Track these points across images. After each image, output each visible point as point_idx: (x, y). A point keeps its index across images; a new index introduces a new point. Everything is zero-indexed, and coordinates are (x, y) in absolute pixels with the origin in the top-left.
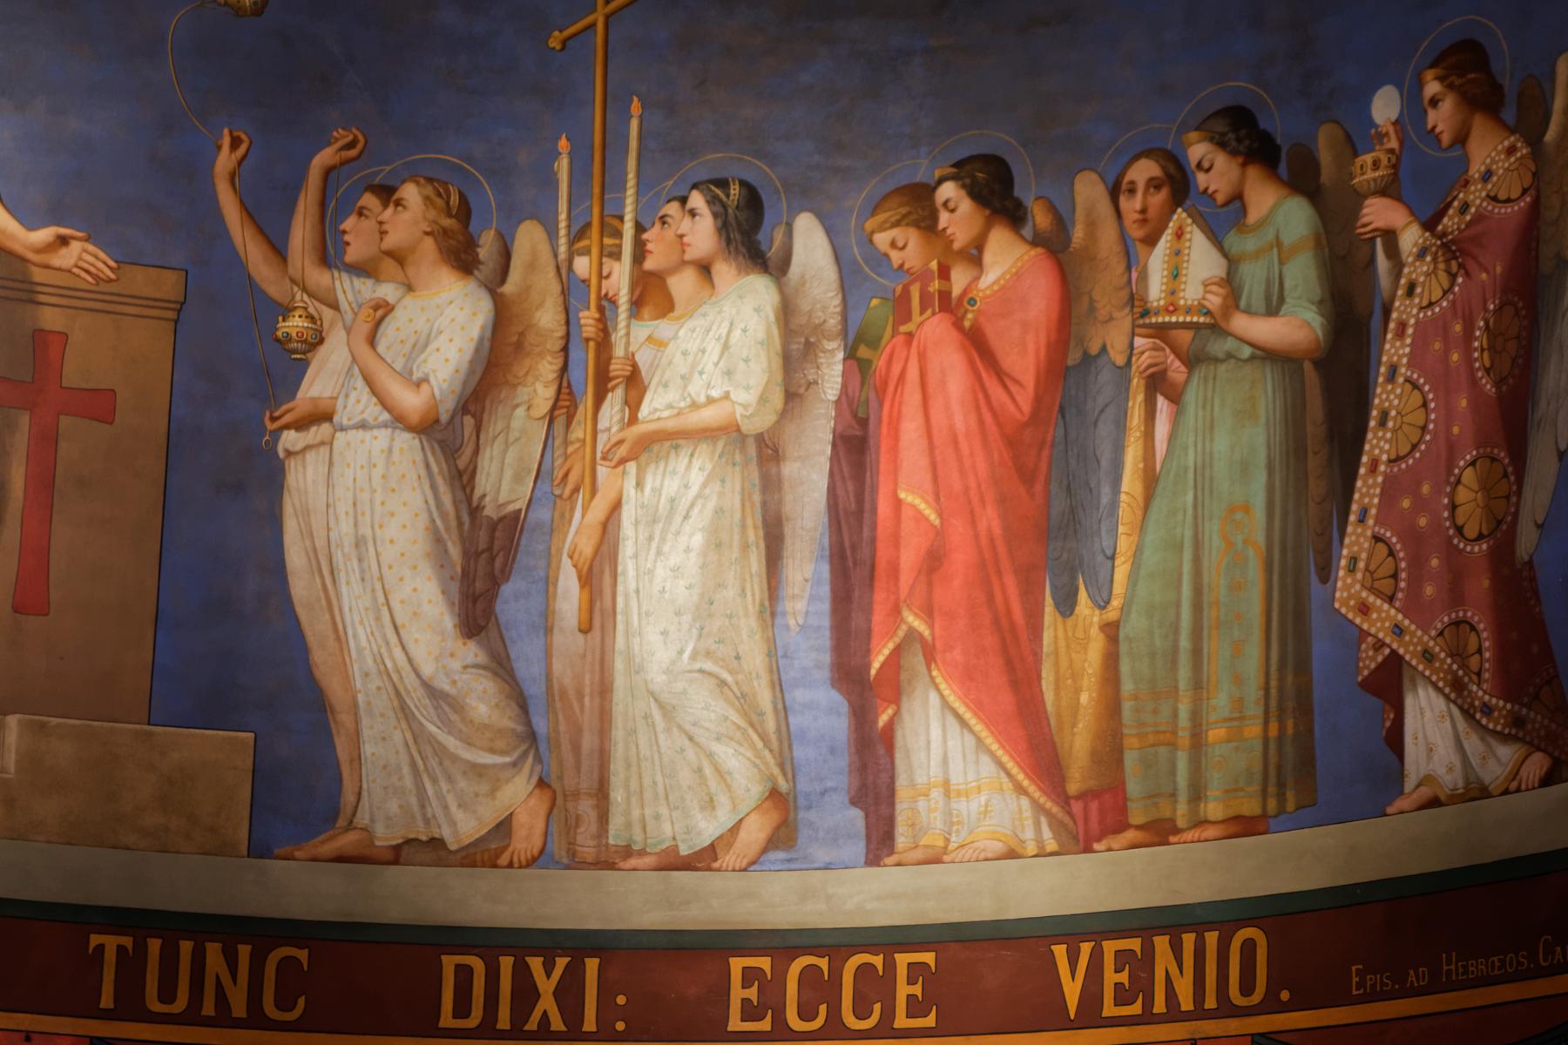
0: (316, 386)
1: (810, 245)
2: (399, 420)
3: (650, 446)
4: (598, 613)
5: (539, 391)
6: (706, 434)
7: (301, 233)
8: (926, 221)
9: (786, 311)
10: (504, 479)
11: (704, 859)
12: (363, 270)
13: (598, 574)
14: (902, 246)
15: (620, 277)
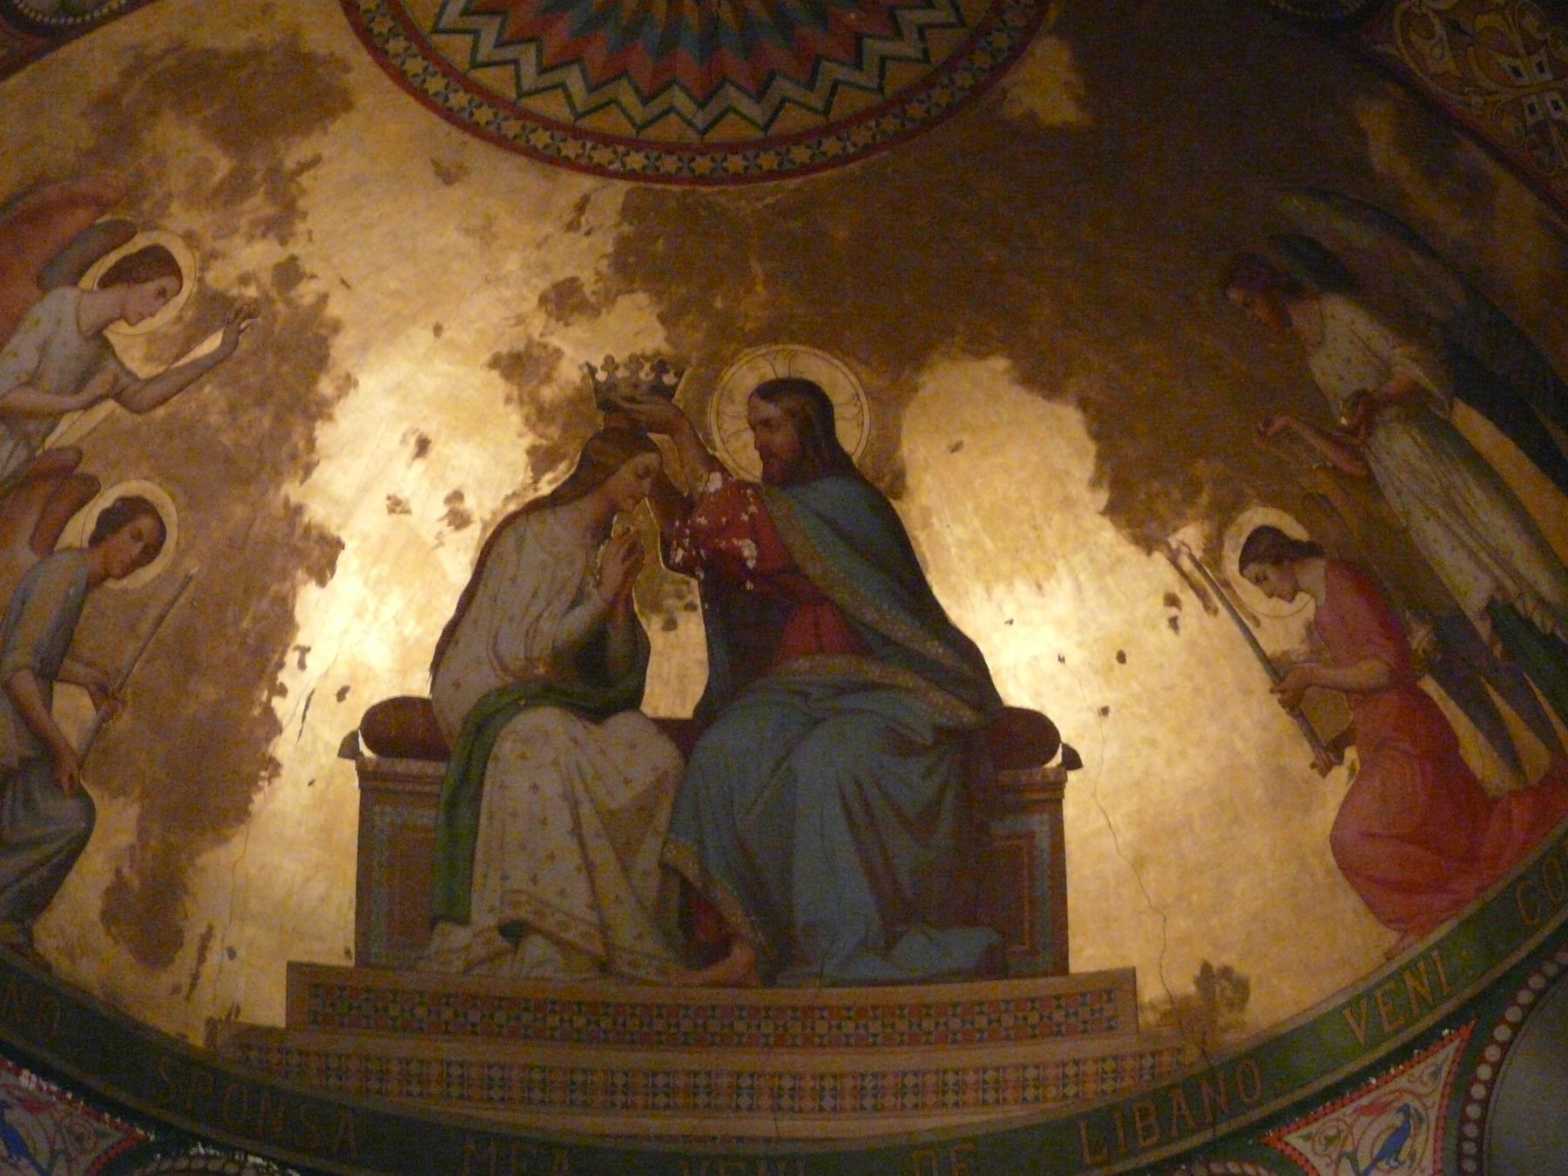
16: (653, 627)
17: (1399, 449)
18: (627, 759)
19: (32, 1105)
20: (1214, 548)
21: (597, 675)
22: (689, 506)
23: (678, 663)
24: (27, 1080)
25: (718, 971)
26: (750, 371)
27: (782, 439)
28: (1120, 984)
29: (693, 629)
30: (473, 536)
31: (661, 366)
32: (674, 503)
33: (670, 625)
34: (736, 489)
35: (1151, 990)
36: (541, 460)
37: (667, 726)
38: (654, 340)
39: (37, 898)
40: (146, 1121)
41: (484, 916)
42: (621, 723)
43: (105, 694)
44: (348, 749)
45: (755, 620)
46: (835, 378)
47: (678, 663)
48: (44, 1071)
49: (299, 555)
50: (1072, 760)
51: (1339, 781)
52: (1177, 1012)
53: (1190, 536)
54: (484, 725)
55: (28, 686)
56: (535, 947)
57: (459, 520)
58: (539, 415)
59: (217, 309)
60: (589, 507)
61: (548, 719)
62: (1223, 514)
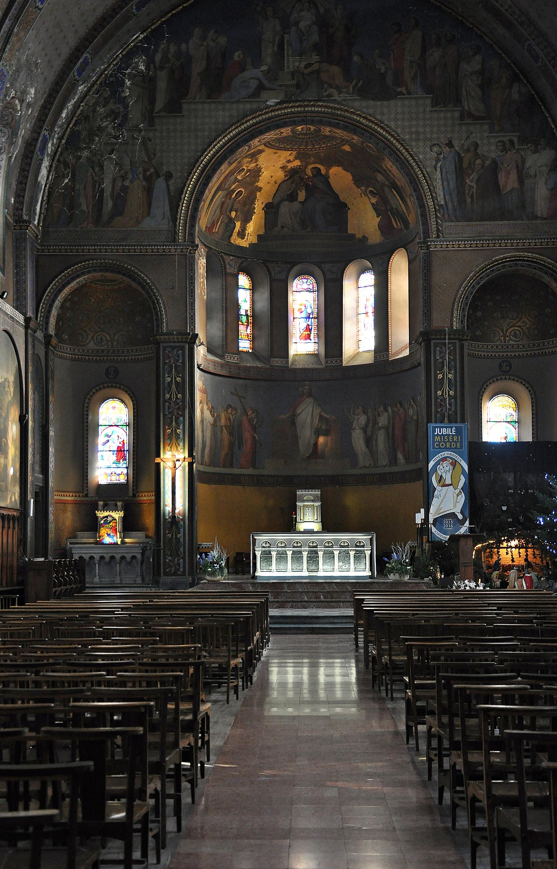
0: (353, 427)
1: (390, 409)
2: (360, 428)
3: (379, 429)
4: (377, 445)
5: (371, 425)
6: (383, 428)
7: (351, 413)
8: (397, 406)
9: (388, 415)
10: (369, 433)
11: (385, 466)
12: (357, 415)
13: (376, 441)
14: (395, 409)
15: (377, 413)
16: (299, 192)
17: (386, 189)
18: (296, 206)
19: (232, 260)
20: (366, 191)
21: (292, 197)
22: (303, 179)
23: (302, 195)
24: (231, 258)
25: (306, 230)
26: (310, 167)
27: (315, 172)
28: (353, 236)
29: (304, 191)
30: (277, 185)
31: (300, 166)
32: (302, 179)
33: (301, 191)
34: (309, 178)
35: (357, 237)
36: (285, 176)
37: (300, 202)
38: (300, 164)
39: (231, 235)
40: (243, 258)
41: (279, 223)
42: (295, 203)
43: (236, 212)
44: (263, 209)
45: (310, 191)
46: (322, 168)
47: (302, 195)
48: (233, 256)
49: (257, 190)
50: (349, 209)
51: (379, 219)
52: (360, 240)
53: (363, 188)
54: (279, 204)
55: (228, 214)
56: (285, 229)
57: (276, 183)
58: (286, 172)
59: (248, 171)
60: (291, 180)
61: (287, 202)
62: (367, 187)
